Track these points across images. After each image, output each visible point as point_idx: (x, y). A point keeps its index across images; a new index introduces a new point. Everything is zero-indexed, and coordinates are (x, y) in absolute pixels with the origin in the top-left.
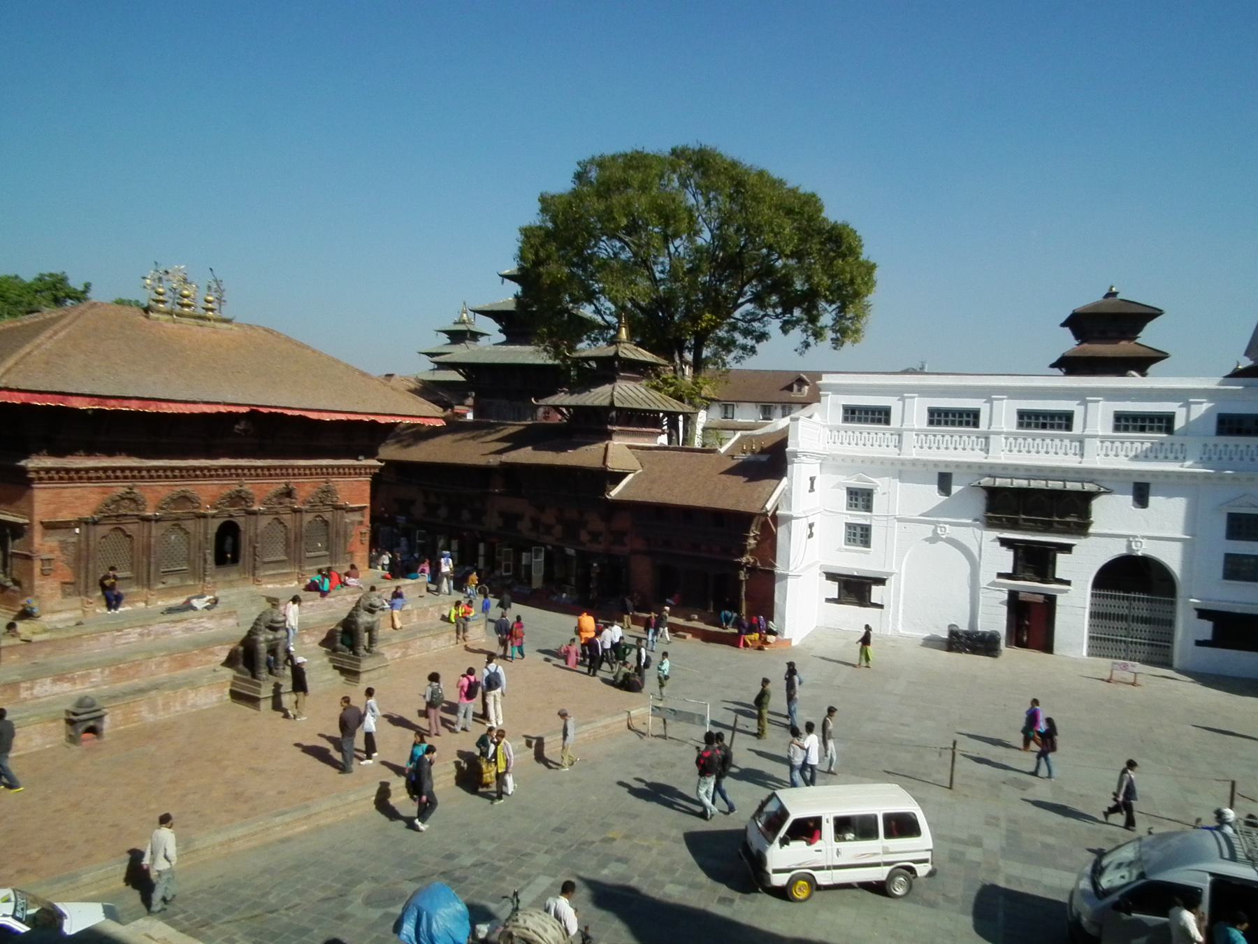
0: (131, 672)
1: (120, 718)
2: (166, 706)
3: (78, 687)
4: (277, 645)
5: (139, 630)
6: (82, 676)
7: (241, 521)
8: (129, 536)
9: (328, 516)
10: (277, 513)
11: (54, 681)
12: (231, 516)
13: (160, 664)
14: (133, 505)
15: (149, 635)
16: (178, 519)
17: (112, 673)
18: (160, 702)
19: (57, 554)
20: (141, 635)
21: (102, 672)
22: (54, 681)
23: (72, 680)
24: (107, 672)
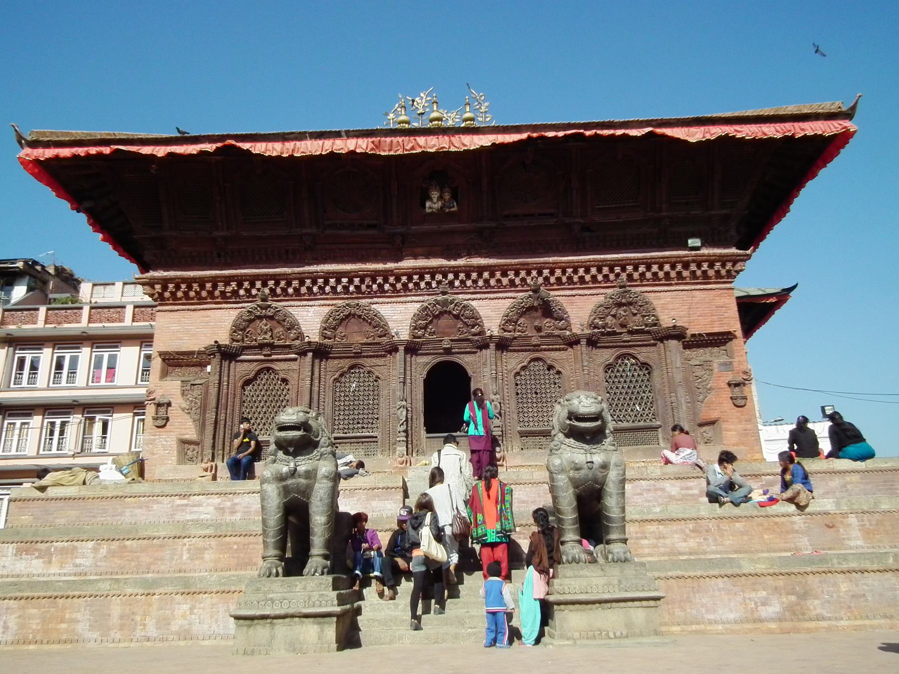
0: (145, 559)
1: (35, 624)
2: (128, 622)
3: (54, 569)
4: (307, 492)
5: (216, 500)
6: (63, 551)
7: (466, 361)
8: (284, 381)
9: (644, 354)
10: (536, 348)
11: (19, 552)
12: (448, 351)
13: (197, 553)
14: (279, 330)
15: (233, 512)
16: (358, 355)
17: (111, 554)
18: (116, 608)
19: (178, 402)
20: (220, 509)
21: (95, 550)
22: (19, 552)
23: (47, 556)
24: (103, 551)
